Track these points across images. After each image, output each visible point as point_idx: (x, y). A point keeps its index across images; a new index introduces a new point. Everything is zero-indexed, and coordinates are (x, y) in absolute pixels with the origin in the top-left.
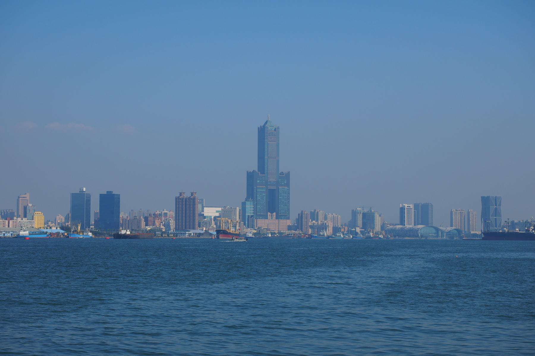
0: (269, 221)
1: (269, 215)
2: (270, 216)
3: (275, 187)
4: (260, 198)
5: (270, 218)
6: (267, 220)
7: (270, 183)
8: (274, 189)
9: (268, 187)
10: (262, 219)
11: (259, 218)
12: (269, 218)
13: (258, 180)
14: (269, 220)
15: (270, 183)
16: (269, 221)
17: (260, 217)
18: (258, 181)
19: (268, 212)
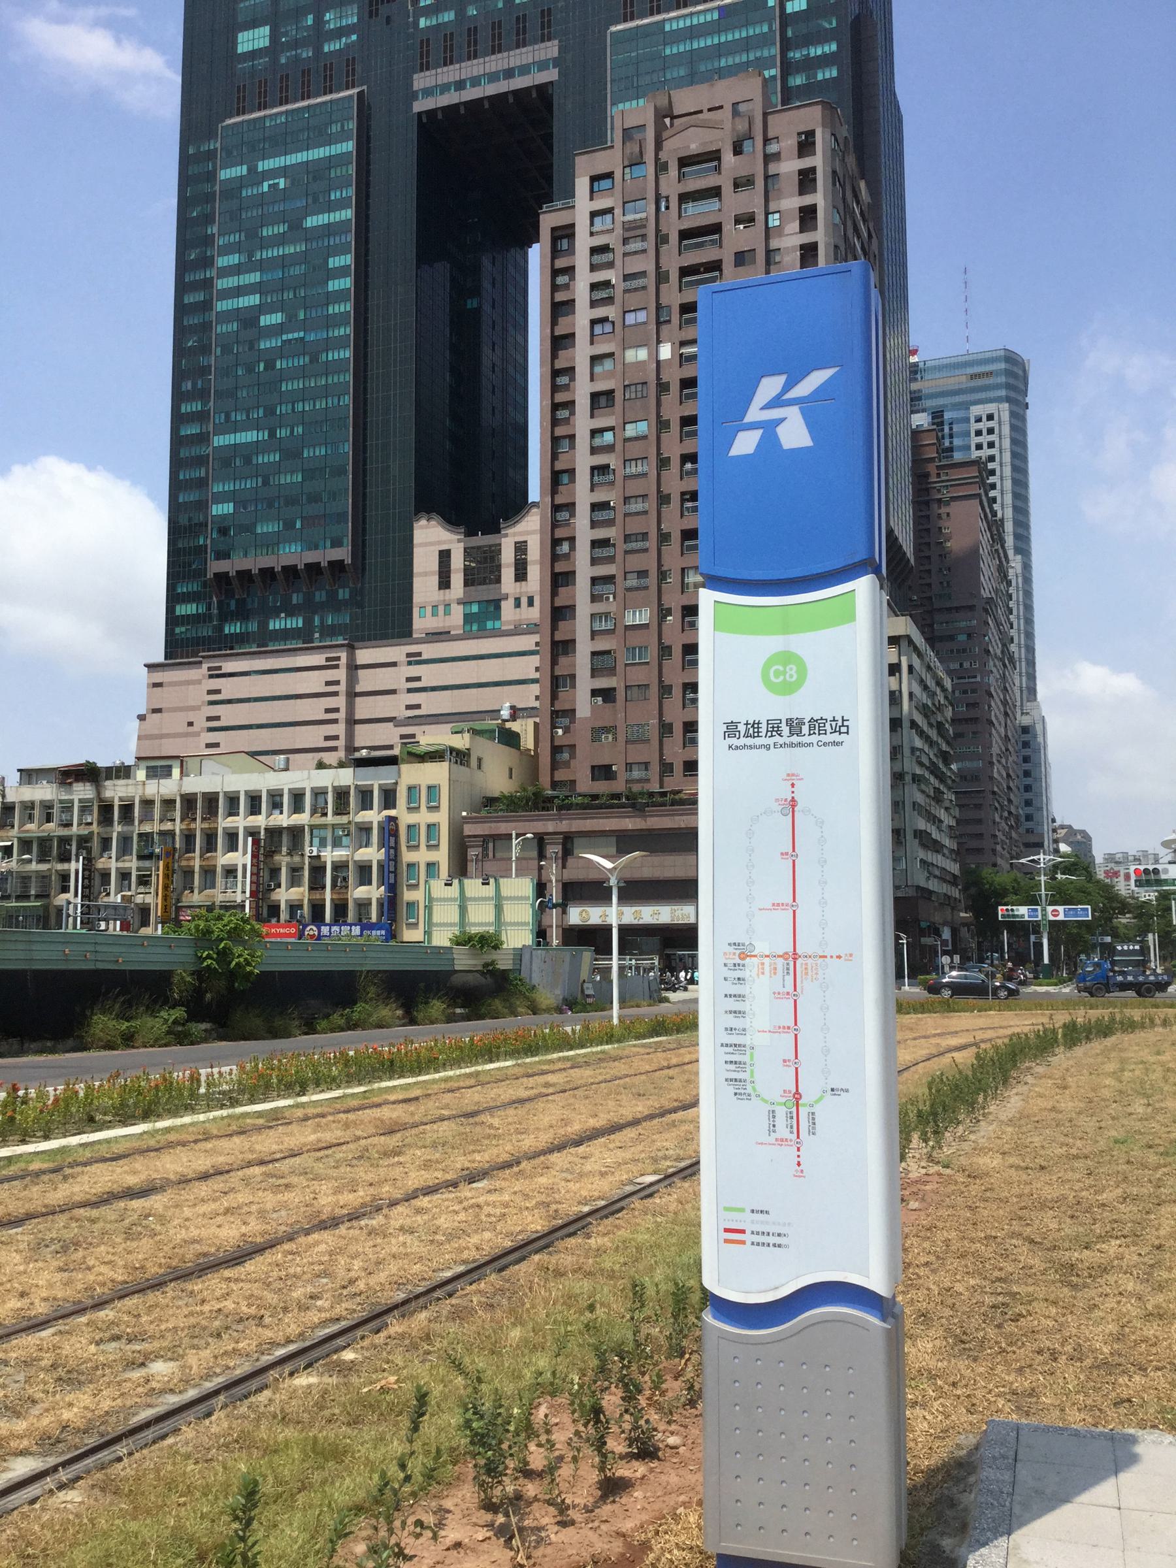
0: (430, 675)
1: (424, 562)
2: (445, 583)
3: (551, 49)
4: (254, 300)
5: (455, 619)
6: (396, 653)
7: (448, 16)
8: (543, 90)
9: (421, 81)
10: (304, 639)
11: (264, 642)
12: (421, 623)
13: (253, 24)
14: (429, 651)
15: (448, 16)
16: (430, 675)
17: (275, 625)
18: (253, 39)
19: (426, 505)
